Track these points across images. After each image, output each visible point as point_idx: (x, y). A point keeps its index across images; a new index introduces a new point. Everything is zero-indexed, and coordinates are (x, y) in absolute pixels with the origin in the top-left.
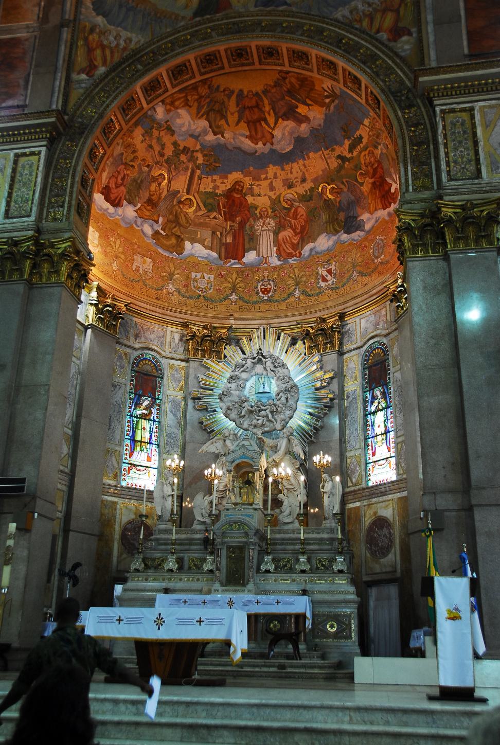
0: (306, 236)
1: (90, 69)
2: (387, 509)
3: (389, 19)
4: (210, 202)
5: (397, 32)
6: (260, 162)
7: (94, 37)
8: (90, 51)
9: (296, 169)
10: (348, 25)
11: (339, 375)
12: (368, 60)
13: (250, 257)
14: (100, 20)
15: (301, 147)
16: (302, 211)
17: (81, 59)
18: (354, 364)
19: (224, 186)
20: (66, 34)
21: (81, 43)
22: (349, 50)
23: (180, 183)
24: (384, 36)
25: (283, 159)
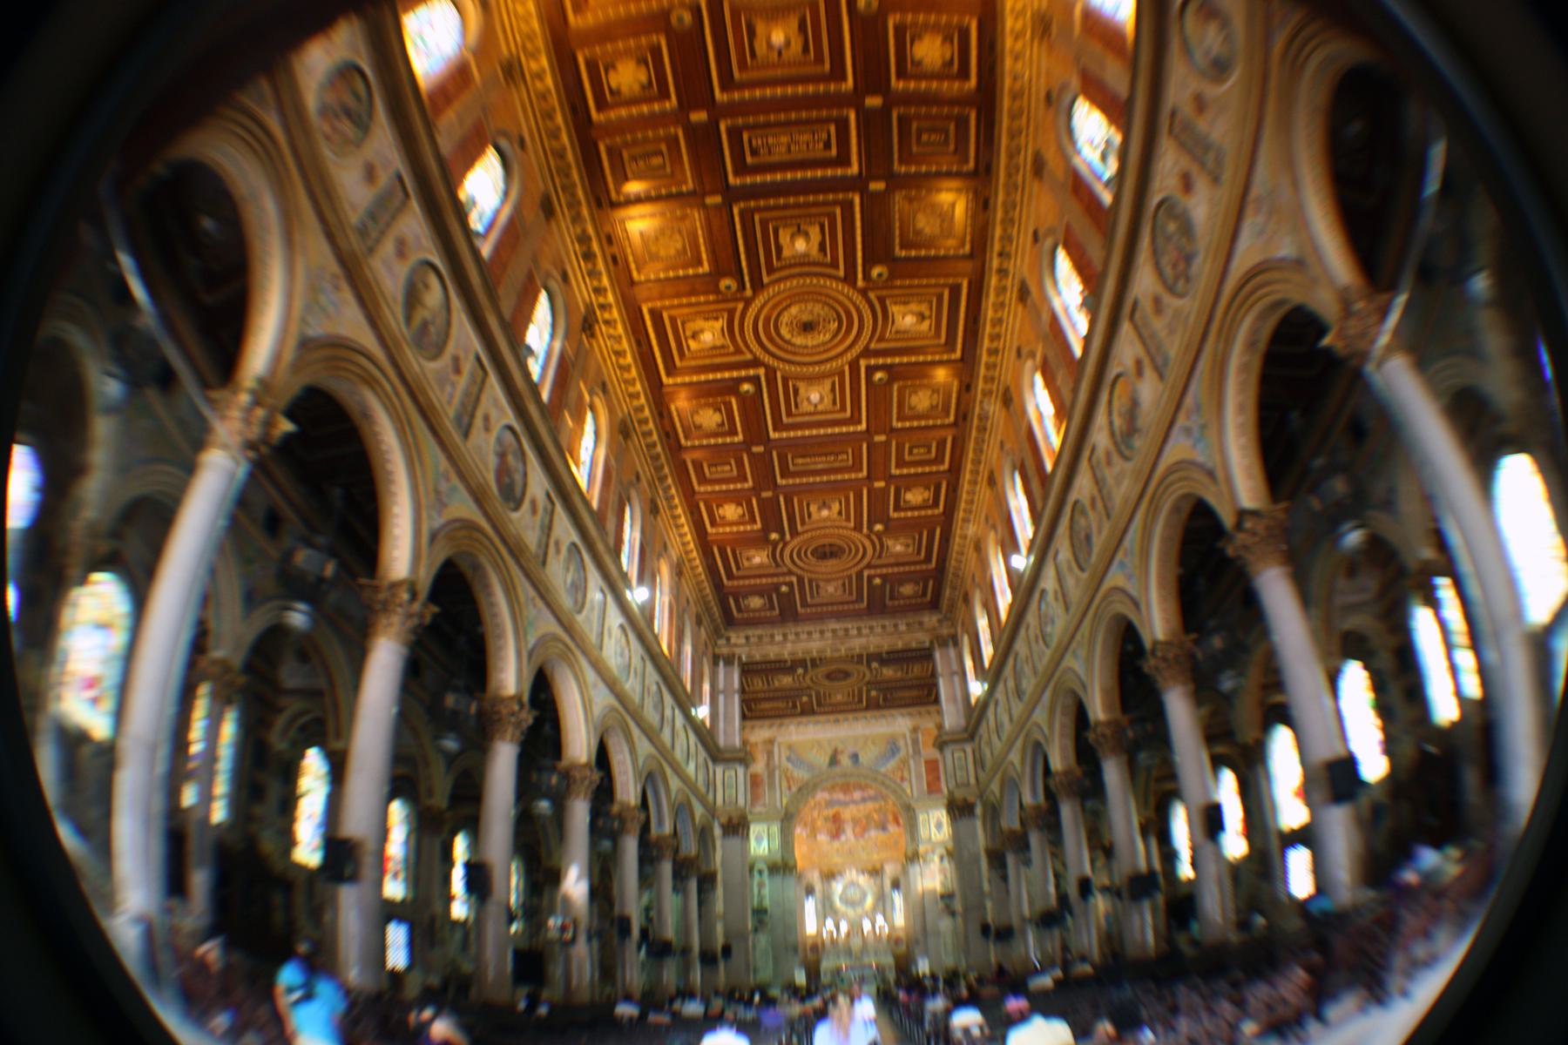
0: (865, 829)
1: (790, 788)
2: (902, 934)
3: (900, 774)
4: (826, 819)
5: (902, 779)
6: (846, 804)
7: (789, 774)
8: (788, 782)
9: (861, 807)
10: (885, 775)
11: (882, 887)
12: (895, 792)
13: (843, 838)
14: (790, 766)
15: (864, 800)
16: (864, 821)
17: (784, 784)
18: (887, 883)
19: (830, 812)
20: (777, 773)
21: (783, 777)
22: (887, 787)
23: (815, 814)
24: (898, 781)
25: (855, 802)
